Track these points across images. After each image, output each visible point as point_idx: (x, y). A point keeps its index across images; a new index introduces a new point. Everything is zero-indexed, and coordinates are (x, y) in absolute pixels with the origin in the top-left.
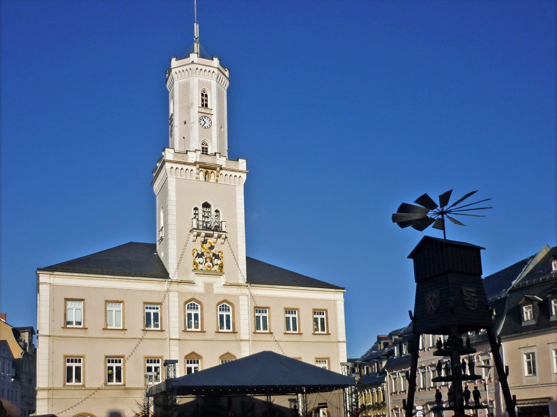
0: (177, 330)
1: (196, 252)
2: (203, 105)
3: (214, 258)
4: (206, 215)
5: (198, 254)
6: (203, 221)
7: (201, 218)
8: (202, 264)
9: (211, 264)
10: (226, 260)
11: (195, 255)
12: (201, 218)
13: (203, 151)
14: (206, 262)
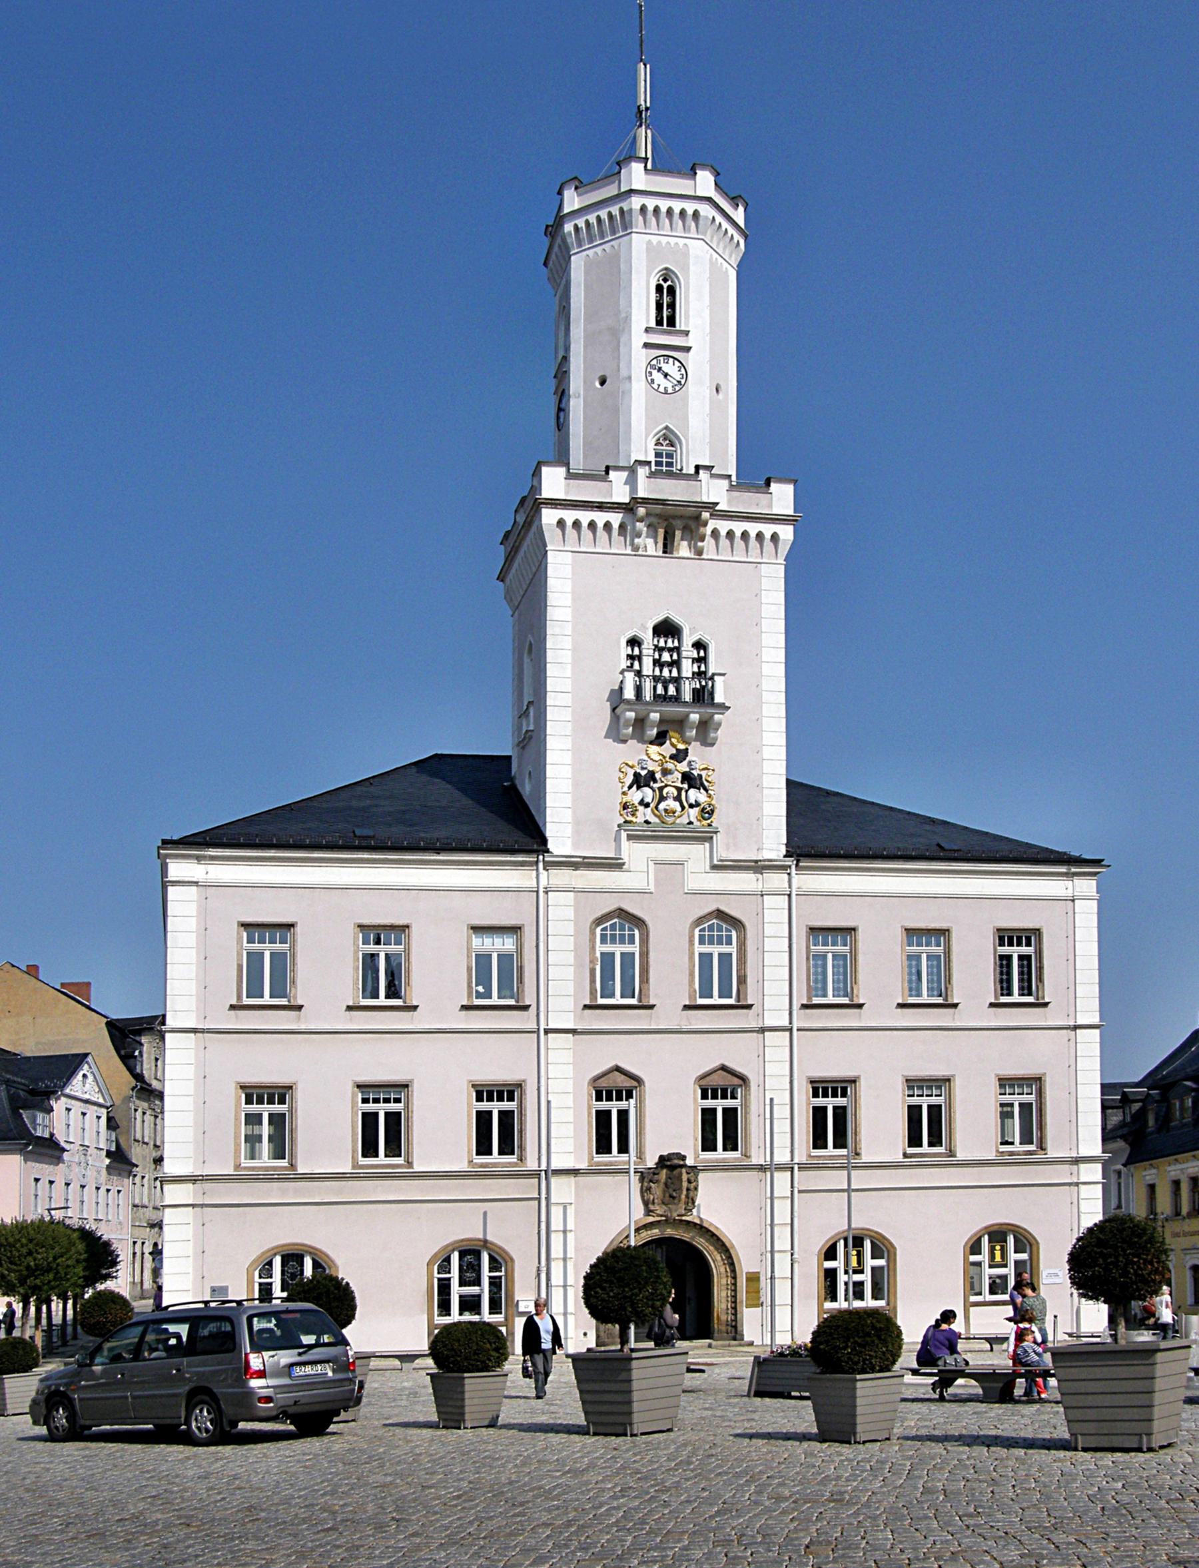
0: (569, 1004)
1: (631, 772)
2: (659, 322)
3: (686, 786)
4: (666, 657)
5: (636, 775)
6: (656, 679)
7: (648, 668)
8: (647, 805)
9: (676, 805)
10: (722, 793)
11: (629, 779)
12: (648, 668)
13: (658, 464)
14: (662, 798)
